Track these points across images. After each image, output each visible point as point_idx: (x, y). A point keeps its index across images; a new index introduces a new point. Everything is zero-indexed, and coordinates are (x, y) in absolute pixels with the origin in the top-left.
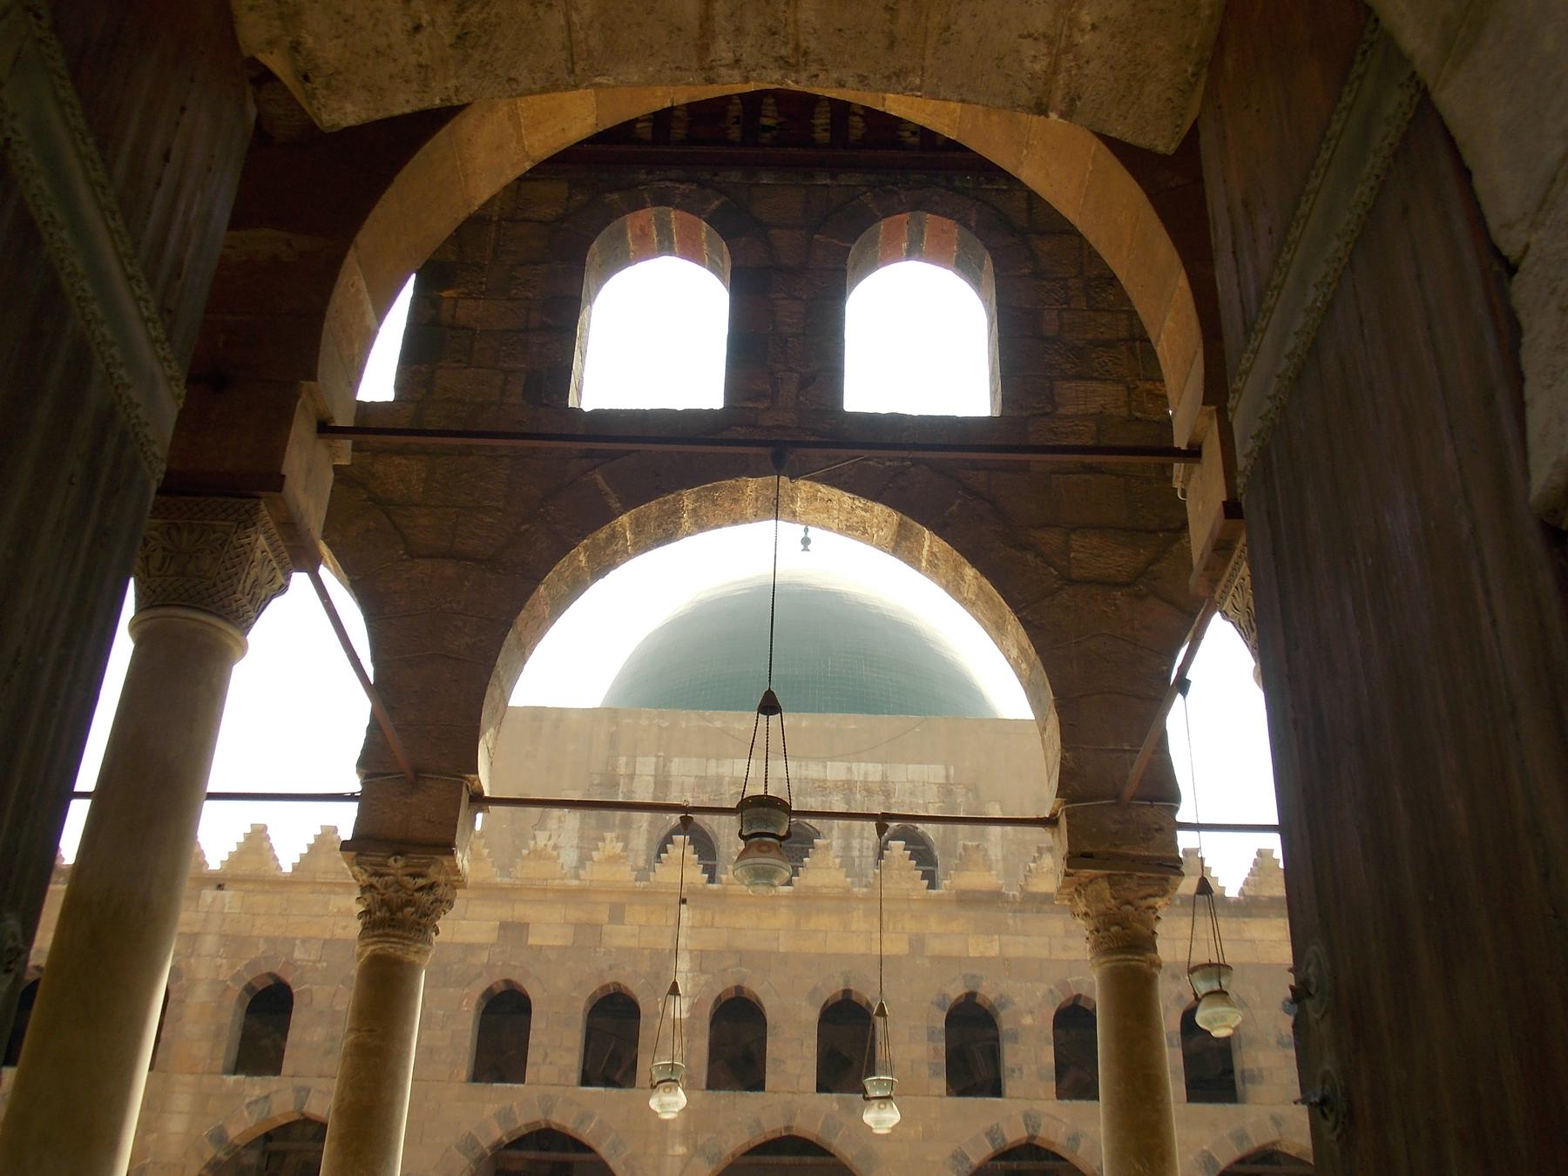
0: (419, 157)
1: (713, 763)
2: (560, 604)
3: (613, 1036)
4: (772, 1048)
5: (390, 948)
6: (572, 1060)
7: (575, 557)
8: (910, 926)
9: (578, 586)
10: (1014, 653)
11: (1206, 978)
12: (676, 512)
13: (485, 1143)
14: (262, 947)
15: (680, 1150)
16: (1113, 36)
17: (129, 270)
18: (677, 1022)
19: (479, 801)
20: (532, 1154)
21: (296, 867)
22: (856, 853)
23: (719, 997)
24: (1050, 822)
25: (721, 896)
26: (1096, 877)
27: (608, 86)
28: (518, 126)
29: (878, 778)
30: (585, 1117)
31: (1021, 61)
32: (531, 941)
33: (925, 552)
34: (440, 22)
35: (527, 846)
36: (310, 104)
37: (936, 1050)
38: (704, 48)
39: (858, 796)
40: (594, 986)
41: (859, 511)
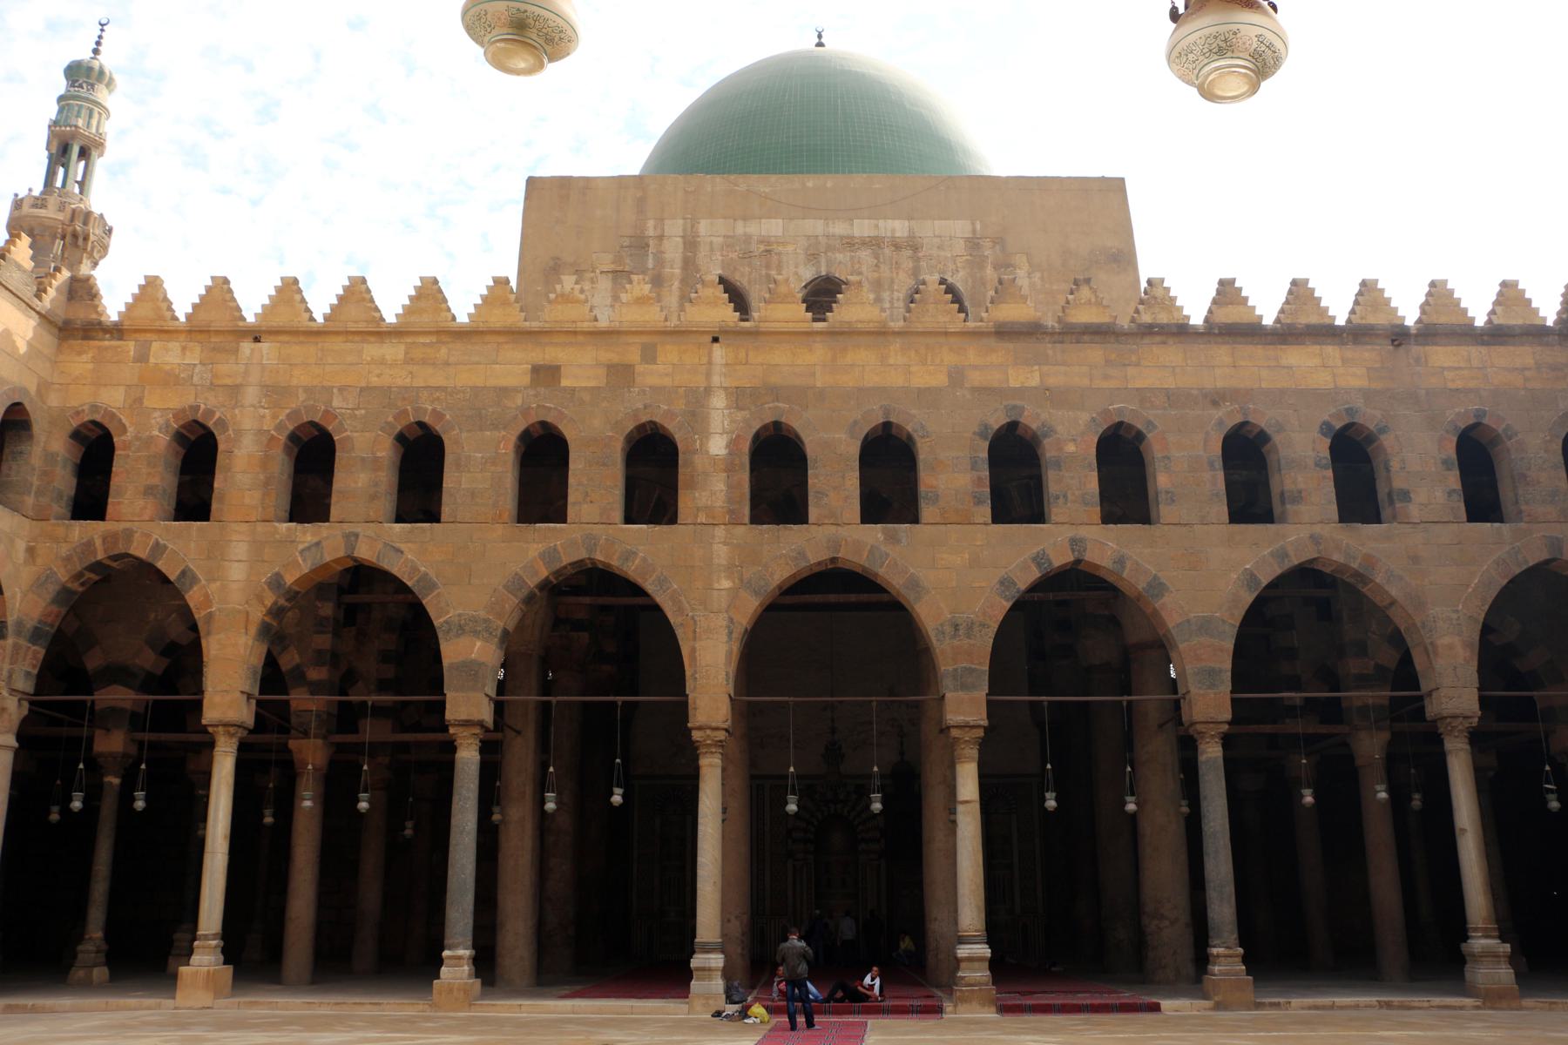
1: (740, 224)
8: (949, 358)
13: (532, 582)
15: (726, 584)
22: (887, 305)
23: (757, 436)
25: (754, 334)
32: (565, 383)
35: (554, 291)
39: (887, 251)
40: (630, 426)
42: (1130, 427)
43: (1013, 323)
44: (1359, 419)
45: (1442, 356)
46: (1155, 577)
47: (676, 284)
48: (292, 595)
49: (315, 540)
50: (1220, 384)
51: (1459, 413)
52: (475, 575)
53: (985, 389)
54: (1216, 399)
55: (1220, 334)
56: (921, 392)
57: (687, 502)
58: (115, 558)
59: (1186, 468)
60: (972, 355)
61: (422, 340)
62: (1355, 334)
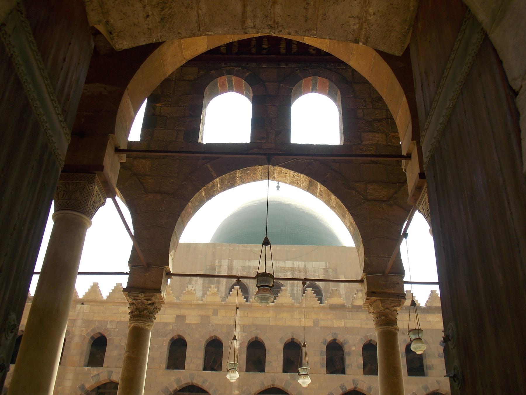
0: (148, 59)
1: (247, 261)
2: (196, 208)
3: (214, 353)
5: (140, 324)
7: (201, 193)
9: (202, 202)
10: (349, 224)
11: (414, 334)
12: (235, 177)
13: (171, 390)
14: (97, 324)
15: (237, 392)
16: (381, 17)
17: (52, 97)
18: (235, 349)
19: (169, 275)
21: (108, 297)
22: (295, 292)
23: (250, 341)
24: (361, 281)
25: (250, 306)
26: (377, 300)
27: (211, 35)
28: (181, 48)
29: (303, 267)
31: (350, 26)
32: (187, 322)
33: (318, 191)
34: (155, 14)
35: (185, 290)
36: (112, 42)
37: (323, 358)
38: (243, 22)
40: (207, 337)
41: (296, 177)
43: (335, 305)
49: (97, 373)
53: (325, 327)
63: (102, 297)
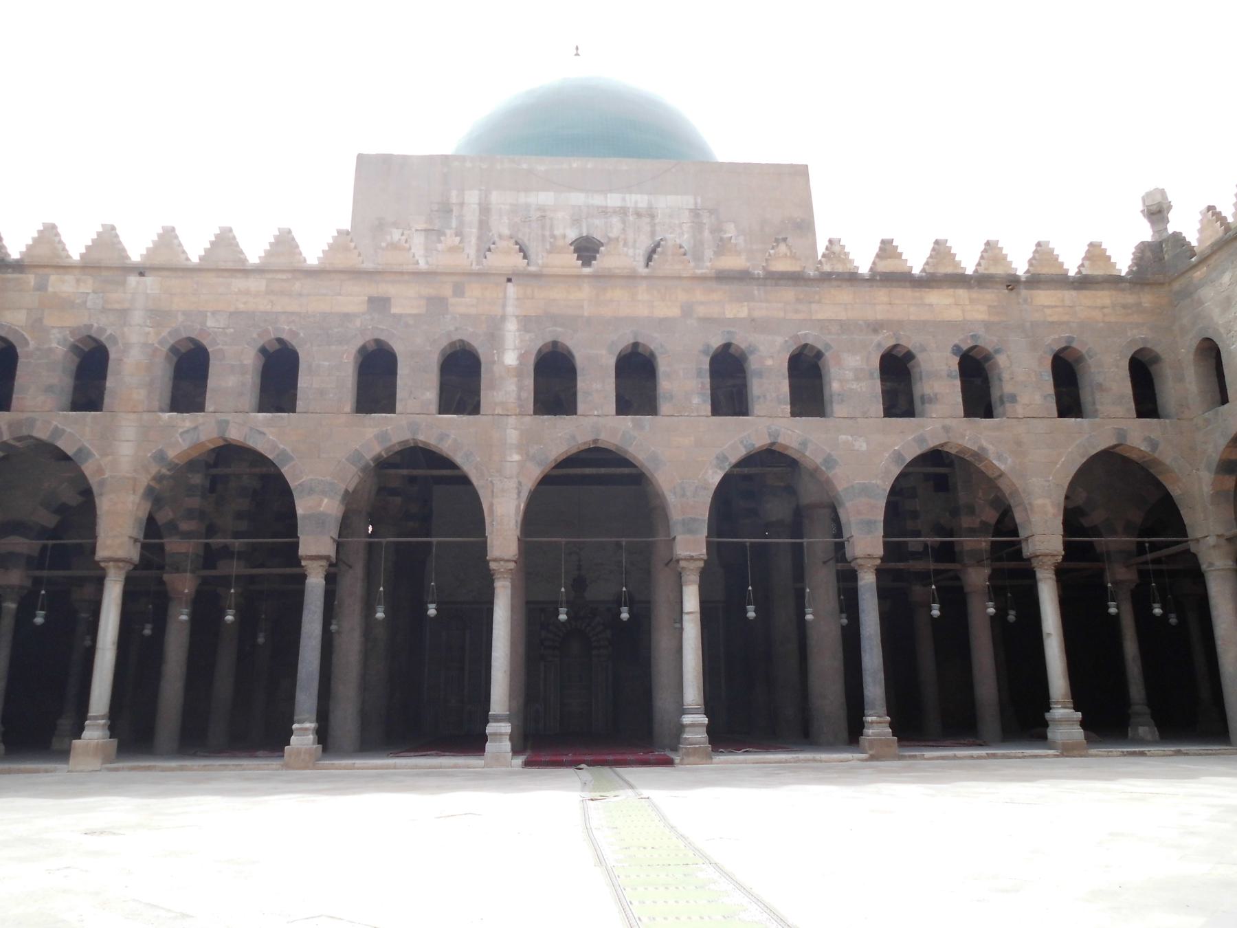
4: (581, 384)
6: (431, 395)
13: (369, 456)
14: (180, 318)
15: (516, 457)
20: (405, 472)
23: (540, 351)
25: (537, 276)
30: (442, 437)
32: (394, 310)
39: (631, 218)
40: (444, 343)
42: (813, 347)
44: (981, 343)
45: (1043, 297)
46: (829, 455)
47: (474, 240)
48: (173, 466)
50: (879, 317)
51: (1053, 341)
52: (324, 455)
54: (876, 327)
55: (881, 280)
56: (662, 321)
57: (487, 398)
58: (19, 439)
59: (853, 377)
60: (699, 295)
61: (279, 276)
62: (980, 281)
63: (188, 259)
